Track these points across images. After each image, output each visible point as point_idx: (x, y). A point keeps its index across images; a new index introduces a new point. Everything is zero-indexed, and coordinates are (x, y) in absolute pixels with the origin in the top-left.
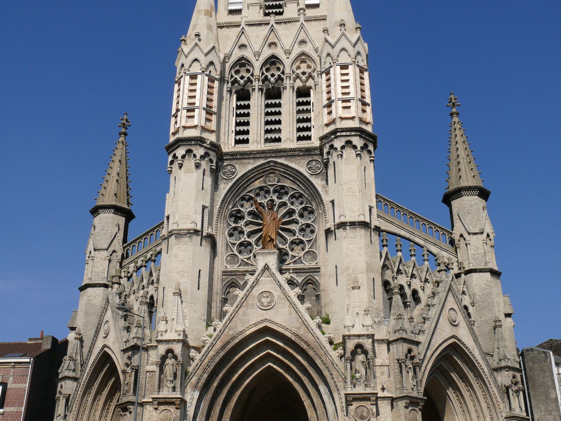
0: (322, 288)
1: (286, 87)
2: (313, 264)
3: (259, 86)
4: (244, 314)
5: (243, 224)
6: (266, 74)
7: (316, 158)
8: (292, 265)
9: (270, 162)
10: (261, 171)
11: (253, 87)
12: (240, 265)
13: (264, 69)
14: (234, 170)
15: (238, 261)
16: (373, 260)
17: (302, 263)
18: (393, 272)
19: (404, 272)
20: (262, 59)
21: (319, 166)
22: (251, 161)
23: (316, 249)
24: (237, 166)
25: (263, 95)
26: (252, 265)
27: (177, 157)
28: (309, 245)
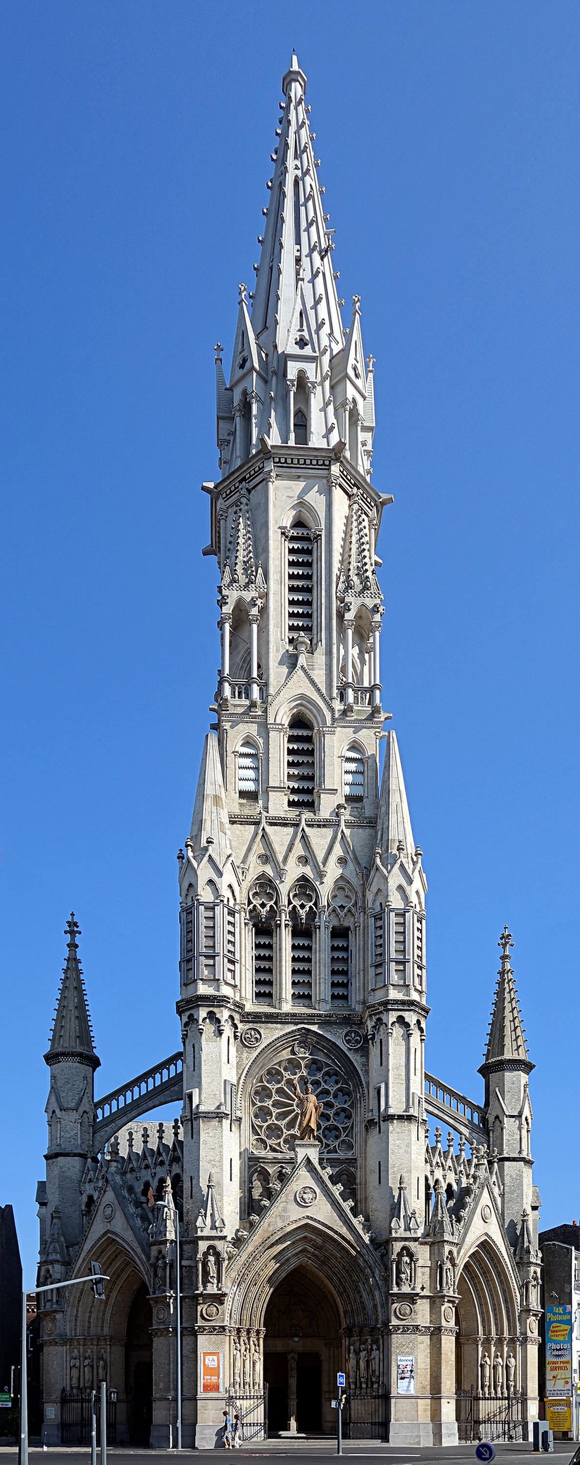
0: (358, 1181)
1: (320, 926)
2: (349, 1155)
3: (285, 920)
5: (271, 1103)
6: (294, 903)
7: (355, 1028)
8: (325, 1154)
9: (302, 1029)
10: (291, 1039)
11: (278, 922)
12: (268, 1151)
13: (291, 895)
14: (259, 1037)
15: (265, 1148)
16: (419, 1157)
17: (336, 1152)
18: (431, 1166)
19: (440, 1165)
21: (359, 1038)
22: (279, 1026)
23: (352, 1138)
24: (262, 1031)
25: (290, 933)
26: (281, 1152)
28: (344, 1132)
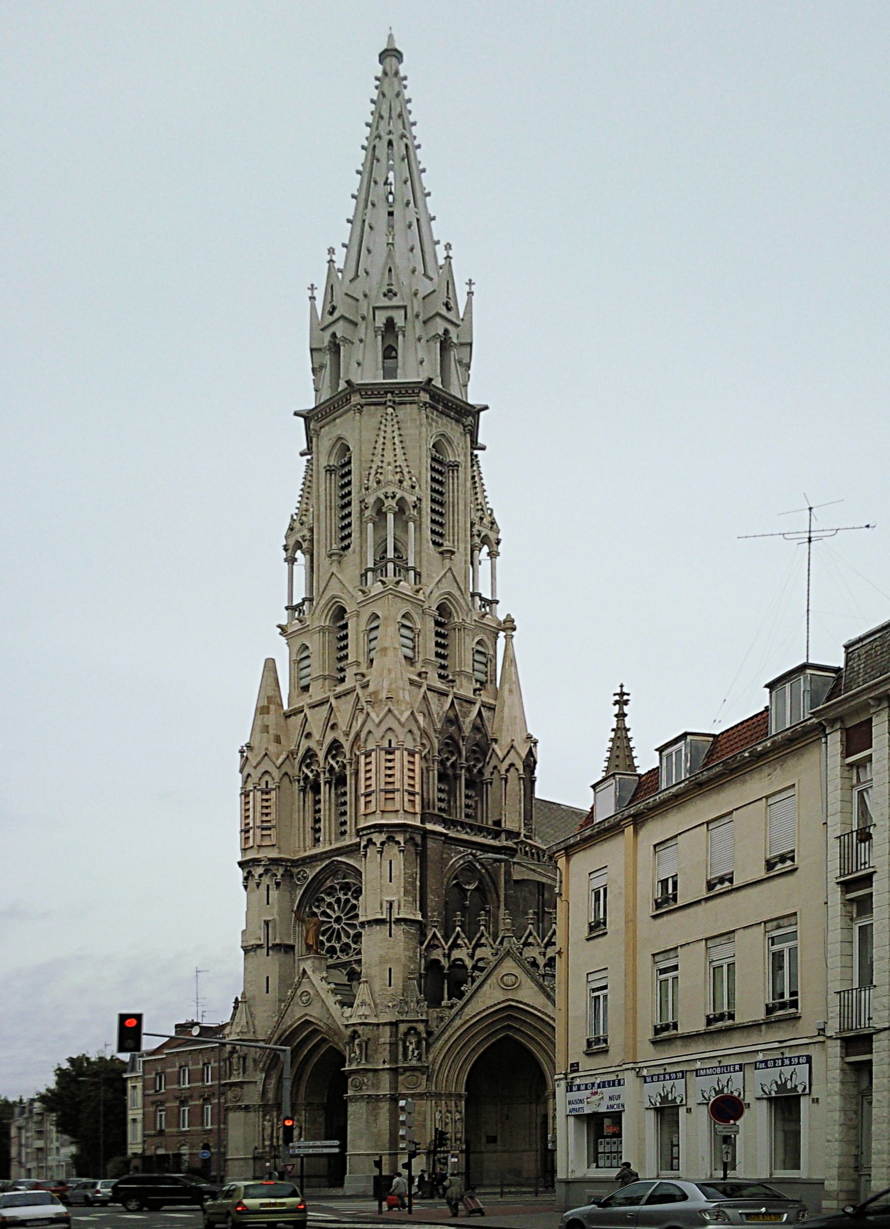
4: (292, 1012)
20: (325, 747)
24: (307, 871)
27: (253, 876)
